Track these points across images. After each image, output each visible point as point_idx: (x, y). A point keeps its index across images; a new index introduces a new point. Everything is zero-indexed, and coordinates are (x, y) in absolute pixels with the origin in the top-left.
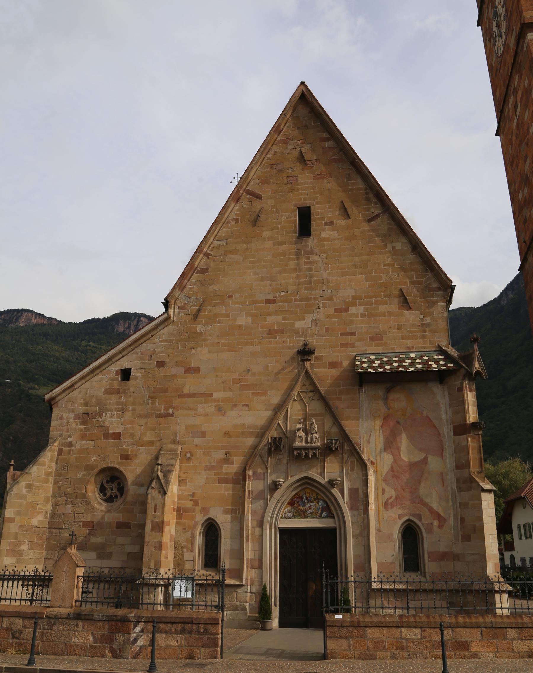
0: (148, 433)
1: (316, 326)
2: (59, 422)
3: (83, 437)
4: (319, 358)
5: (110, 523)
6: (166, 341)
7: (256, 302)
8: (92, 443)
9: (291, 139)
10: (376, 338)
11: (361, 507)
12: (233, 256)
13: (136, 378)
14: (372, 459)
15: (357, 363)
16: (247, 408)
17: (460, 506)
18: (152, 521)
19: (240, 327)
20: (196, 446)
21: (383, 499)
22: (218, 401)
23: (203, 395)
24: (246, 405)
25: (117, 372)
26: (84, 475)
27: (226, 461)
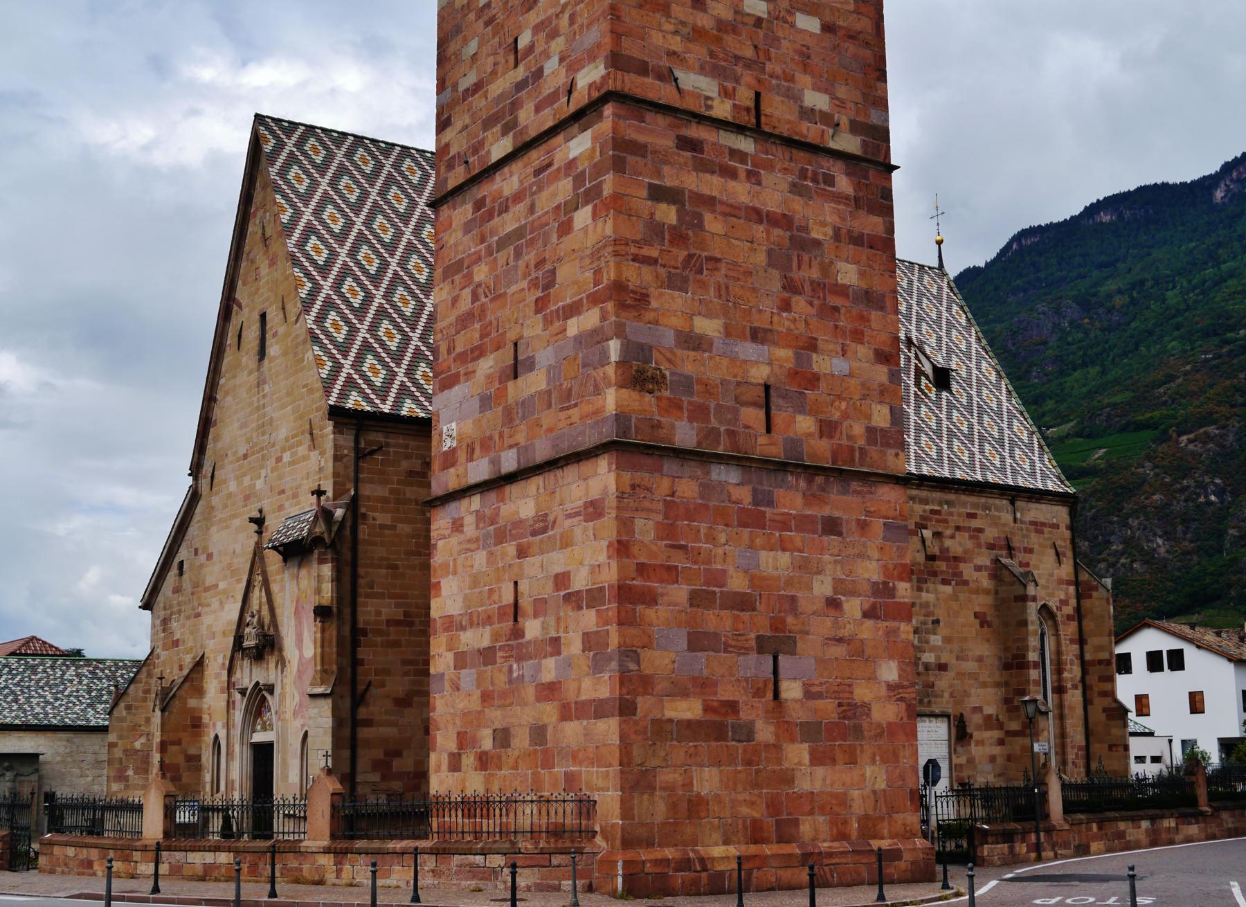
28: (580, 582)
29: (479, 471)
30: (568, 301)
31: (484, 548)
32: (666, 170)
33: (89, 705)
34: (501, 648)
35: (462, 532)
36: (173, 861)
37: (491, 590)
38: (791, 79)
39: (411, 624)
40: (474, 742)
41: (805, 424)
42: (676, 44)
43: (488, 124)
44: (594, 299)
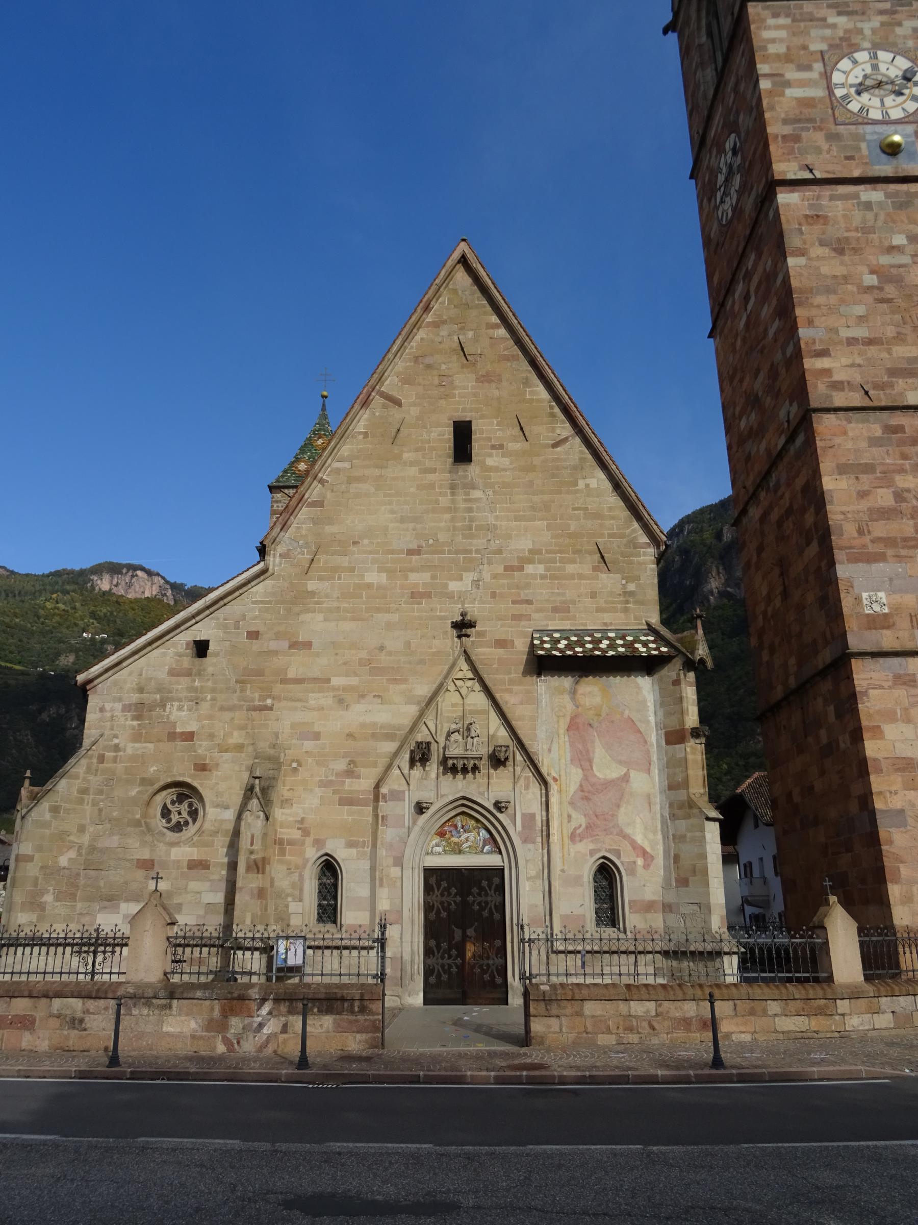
0: (236, 733)
1: (478, 588)
2: (98, 715)
3: (137, 737)
4: (481, 634)
5: (178, 861)
6: (262, 602)
7: (392, 552)
8: (151, 746)
9: (444, 322)
10: (561, 609)
11: (539, 839)
12: (360, 485)
13: (217, 655)
14: (554, 774)
15: (536, 642)
16: (379, 701)
17: (674, 839)
18: (248, 858)
19: (369, 586)
20: (307, 752)
21: (568, 829)
22: (338, 689)
23: (315, 680)
24: (379, 696)
25: (188, 644)
26: (137, 792)
27: (350, 773)
36: (897, 1009)
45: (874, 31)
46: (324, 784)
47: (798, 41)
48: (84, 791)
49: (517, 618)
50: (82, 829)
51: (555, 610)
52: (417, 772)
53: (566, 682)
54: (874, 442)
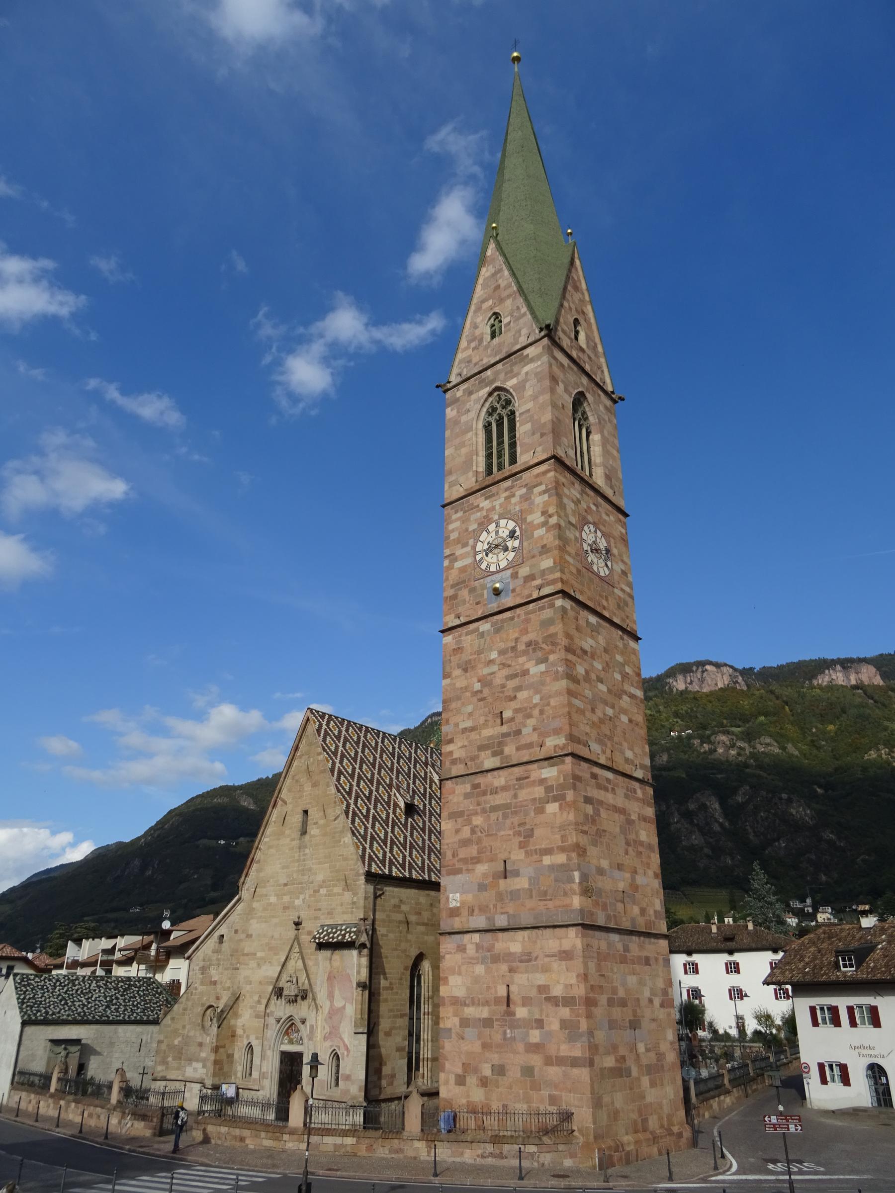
3: (202, 984)
7: (280, 885)
10: (330, 914)
28: (557, 991)
29: (480, 922)
30: (543, 846)
31: (482, 963)
32: (588, 788)
33: (108, 1007)
34: (497, 1020)
35: (465, 952)
37: (488, 988)
38: (621, 745)
39: (392, 989)
40: (476, 1070)
41: (636, 910)
42: (588, 729)
43: (482, 748)
44: (562, 849)
45: (501, 505)
46: (251, 1007)
47: (464, 527)
48: (185, 1009)
49: (316, 918)
50: (184, 1027)
51: (329, 913)
52: (279, 1002)
53: (327, 953)
54: (467, 796)
